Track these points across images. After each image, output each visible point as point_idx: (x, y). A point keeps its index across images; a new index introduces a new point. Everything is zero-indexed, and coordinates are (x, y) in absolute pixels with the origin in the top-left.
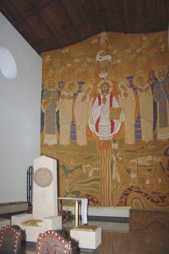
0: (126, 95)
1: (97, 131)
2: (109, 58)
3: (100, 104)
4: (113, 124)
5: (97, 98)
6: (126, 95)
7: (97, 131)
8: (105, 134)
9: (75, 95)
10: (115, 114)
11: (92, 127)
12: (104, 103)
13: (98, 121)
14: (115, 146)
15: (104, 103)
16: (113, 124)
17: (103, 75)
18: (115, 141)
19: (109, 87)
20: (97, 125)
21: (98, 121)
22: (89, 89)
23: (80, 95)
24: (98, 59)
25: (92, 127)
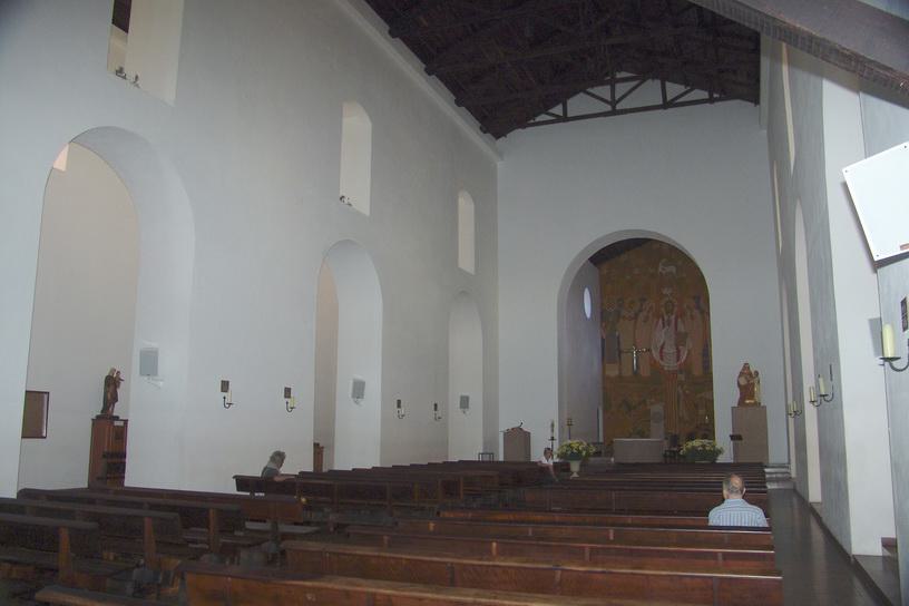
0: (692, 318)
1: (662, 359)
2: (673, 269)
3: (664, 327)
4: (678, 351)
5: (661, 321)
6: (692, 318)
7: (662, 359)
8: (670, 364)
9: (636, 315)
10: (680, 340)
11: (656, 354)
12: (669, 325)
13: (662, 348)
14: (682, 377)
15: (669, 325)
16: (678, 351)
17: (666, 291)
18: (681, 372)
19: (673, 305)
20: (661, 352)
21: (662, 348)
22: (651, 308)
23: (642, 316)
24: (660, 268)
25: (656, 354)
